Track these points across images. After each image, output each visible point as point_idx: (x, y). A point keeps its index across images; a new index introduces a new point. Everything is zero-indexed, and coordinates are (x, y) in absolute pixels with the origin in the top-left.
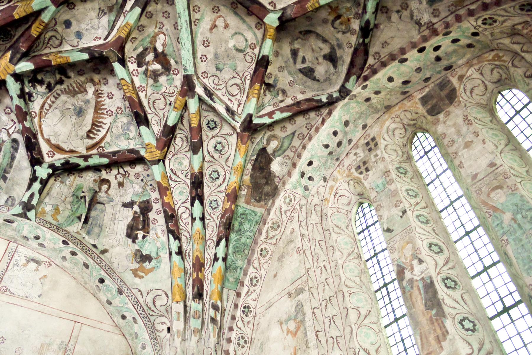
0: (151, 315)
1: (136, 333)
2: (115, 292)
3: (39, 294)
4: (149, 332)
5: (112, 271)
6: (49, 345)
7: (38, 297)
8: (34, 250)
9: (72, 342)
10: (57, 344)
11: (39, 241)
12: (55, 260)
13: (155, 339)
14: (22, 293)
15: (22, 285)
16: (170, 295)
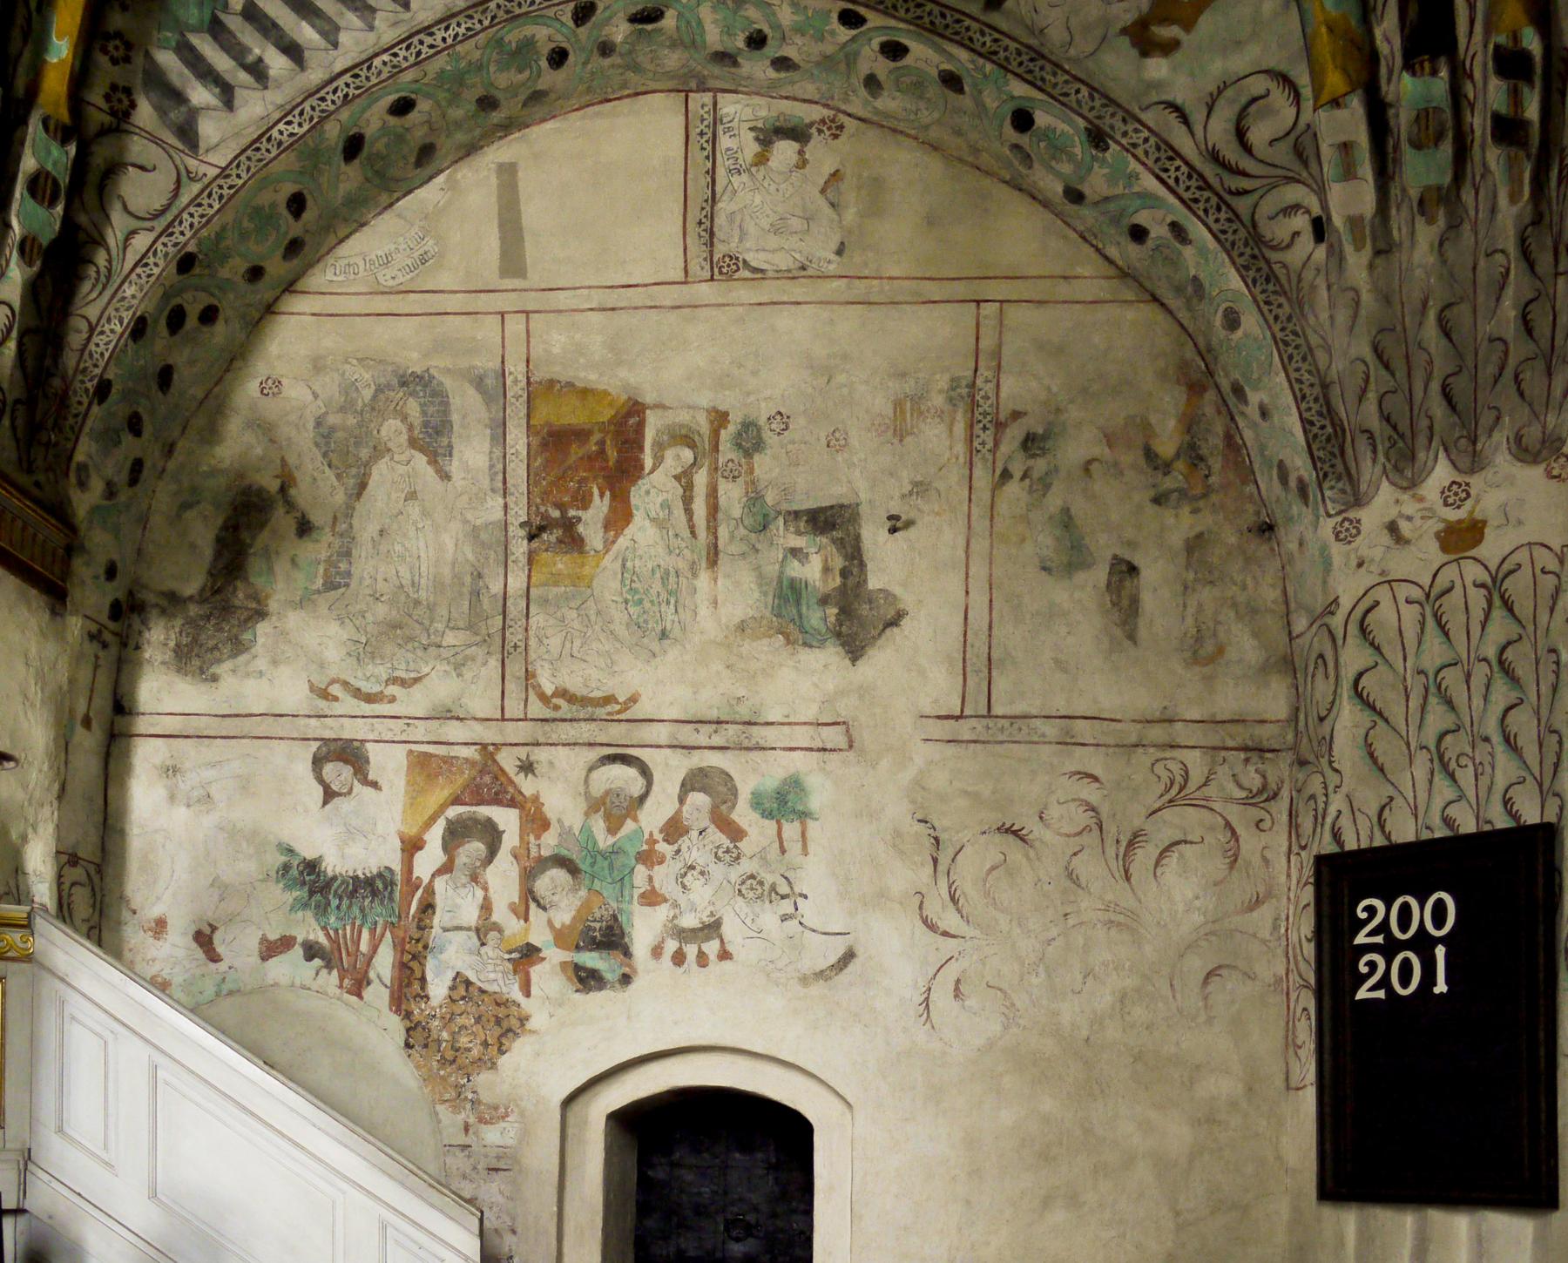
0: (1240, 193)
1: (1195, 278)
2: (1079, 147)
3: (834, 246)
4: (1240, 261)
5: (1049, 67)
6: (917, 399)
7: (833, 257)
8: (768, 91)
9: (984, 373)
10: (940, 391)
11: (771, 50)
12: (846, 100)
13: (1268, 280)
14: (783, 262)
15: (776, 230)
16: (1303, 80)
